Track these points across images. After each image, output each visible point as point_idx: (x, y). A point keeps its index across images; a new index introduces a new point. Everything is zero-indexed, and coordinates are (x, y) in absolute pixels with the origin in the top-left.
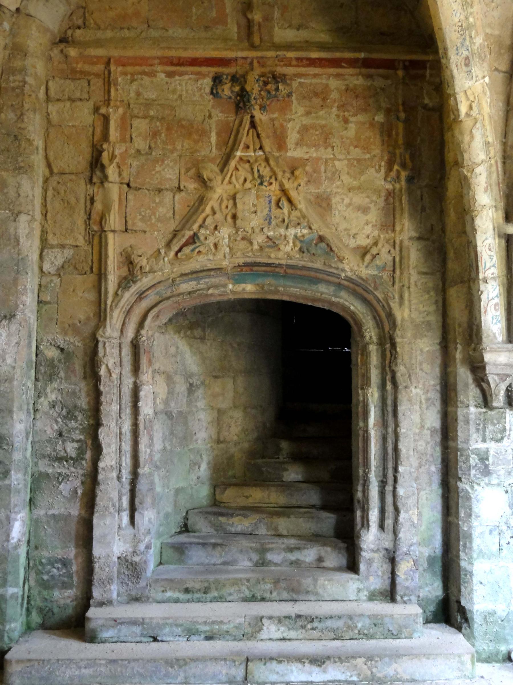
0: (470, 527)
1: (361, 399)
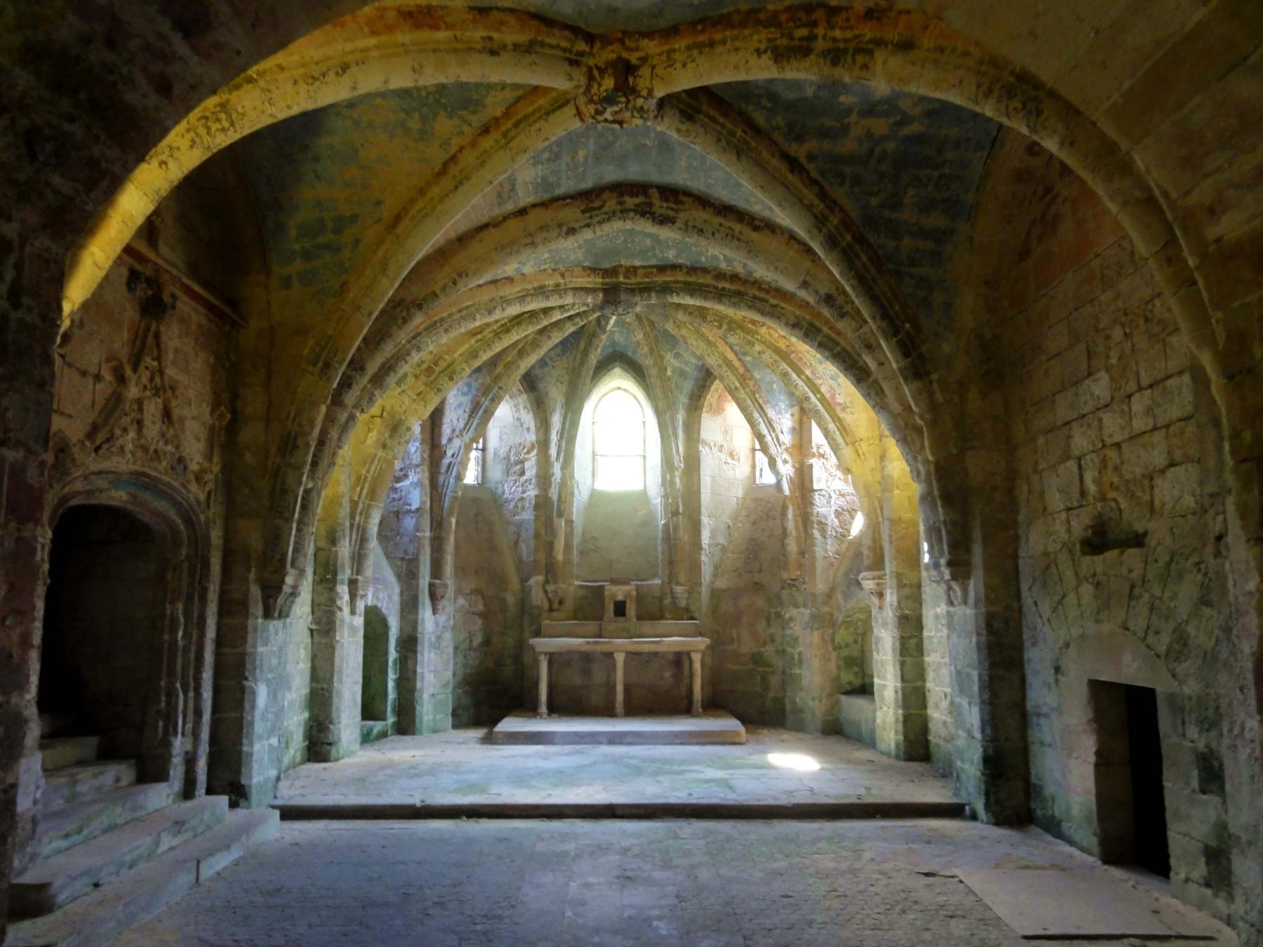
0: (253, 716)
1: (168, 612)
